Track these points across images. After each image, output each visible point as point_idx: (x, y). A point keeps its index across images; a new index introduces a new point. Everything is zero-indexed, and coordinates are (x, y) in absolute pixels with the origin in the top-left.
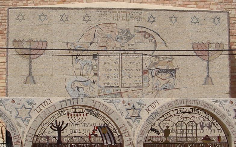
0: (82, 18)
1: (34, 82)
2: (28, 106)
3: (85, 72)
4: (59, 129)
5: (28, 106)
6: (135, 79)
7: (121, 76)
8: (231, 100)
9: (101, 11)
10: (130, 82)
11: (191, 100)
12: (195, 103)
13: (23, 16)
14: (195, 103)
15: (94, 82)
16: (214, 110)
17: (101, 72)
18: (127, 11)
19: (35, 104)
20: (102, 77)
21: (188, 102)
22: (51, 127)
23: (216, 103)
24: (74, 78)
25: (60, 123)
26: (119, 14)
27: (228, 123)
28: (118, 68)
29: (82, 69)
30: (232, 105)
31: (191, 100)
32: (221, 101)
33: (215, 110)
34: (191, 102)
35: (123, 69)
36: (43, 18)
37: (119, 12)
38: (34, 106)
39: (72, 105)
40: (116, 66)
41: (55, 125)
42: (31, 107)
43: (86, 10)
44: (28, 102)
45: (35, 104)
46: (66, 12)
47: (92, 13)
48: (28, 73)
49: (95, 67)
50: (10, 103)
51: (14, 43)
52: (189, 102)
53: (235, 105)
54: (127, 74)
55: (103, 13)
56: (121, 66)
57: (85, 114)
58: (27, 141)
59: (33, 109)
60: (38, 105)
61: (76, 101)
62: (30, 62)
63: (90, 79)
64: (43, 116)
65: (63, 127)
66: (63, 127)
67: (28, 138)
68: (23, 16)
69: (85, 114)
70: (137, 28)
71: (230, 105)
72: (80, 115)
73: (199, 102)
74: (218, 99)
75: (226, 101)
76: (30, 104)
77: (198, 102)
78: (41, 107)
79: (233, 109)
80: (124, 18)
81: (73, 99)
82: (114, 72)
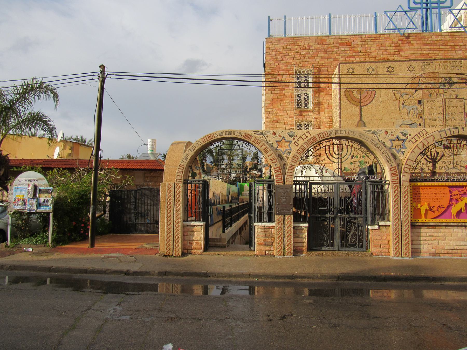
0: (407, 69)
1: (365, 126)
2: (402, 137)
3: (411, 116)
4: (434, 161)
5: (403, 137)
6: (460, 121)
7: (445, 119)
9: (425, 62)
10: (453, 124)
13: (353, 69)
15: (420, 125)
17: (426, 115)
18: (448, 61)
19: (410, 135)
20: (427, 120)
22: (425, 159)
24: (402, 122)
25: (435, 154)
26: (441, 65)
28: (442, 112)
29: (408, 113)
35: (447, 113)
36: (371, 70)
37: (441, 62)
38: (409, 137)
39: (453, 134)
40: (441, 110)
41: (430, 157)
42: (405, 138)
43: (410, 62)
44: (402, 133)
45: (410, 135)
46: (391, 64)
47: (415, 64)
48: (359, 118)
49: (420, 111)
50: (384, 134)
51: (346, 93)
54: (451, 117)
55: (426, 64)
56: (444, 110)
57: (462, 145)
58: (405, 172)
59: (408, 140)
60: (412, 136)
61: (456, 131)
62: (361, 109)
63: (416, 121)
64: (421, 146)
65: (438, 158)
66: (438, 158)
67: (405, 169)
68: (353, 69)
69: (462, 145)
70: (459, 76)
72: (457, 146)
76: (405, 134)
78: (416, 137)
80: (446, 67)
81: (453, 128)
82: (439, 116)
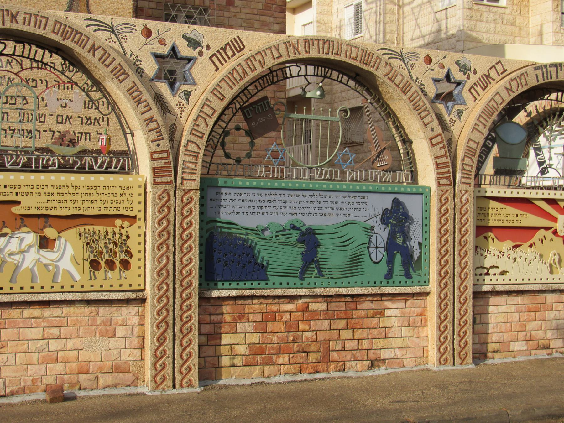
8: (145, 27)
11: (18, 13)
12: (32, 23)
14: (32, 23)
16: (93, 49)
21: (8, 19)
23: (100, 32)
27: (135, 94)
30: (148, 40)
31: (18, 13)
32: (115, 25)
33: (95, 50)
34: (20, 18)
52: (14, 17)
53: (157, 40)
71: (144, 39)
73: (44, 20)
74: (107, 19)
75: (131, 28)
77: (41, 21)
79: (152, 53)
